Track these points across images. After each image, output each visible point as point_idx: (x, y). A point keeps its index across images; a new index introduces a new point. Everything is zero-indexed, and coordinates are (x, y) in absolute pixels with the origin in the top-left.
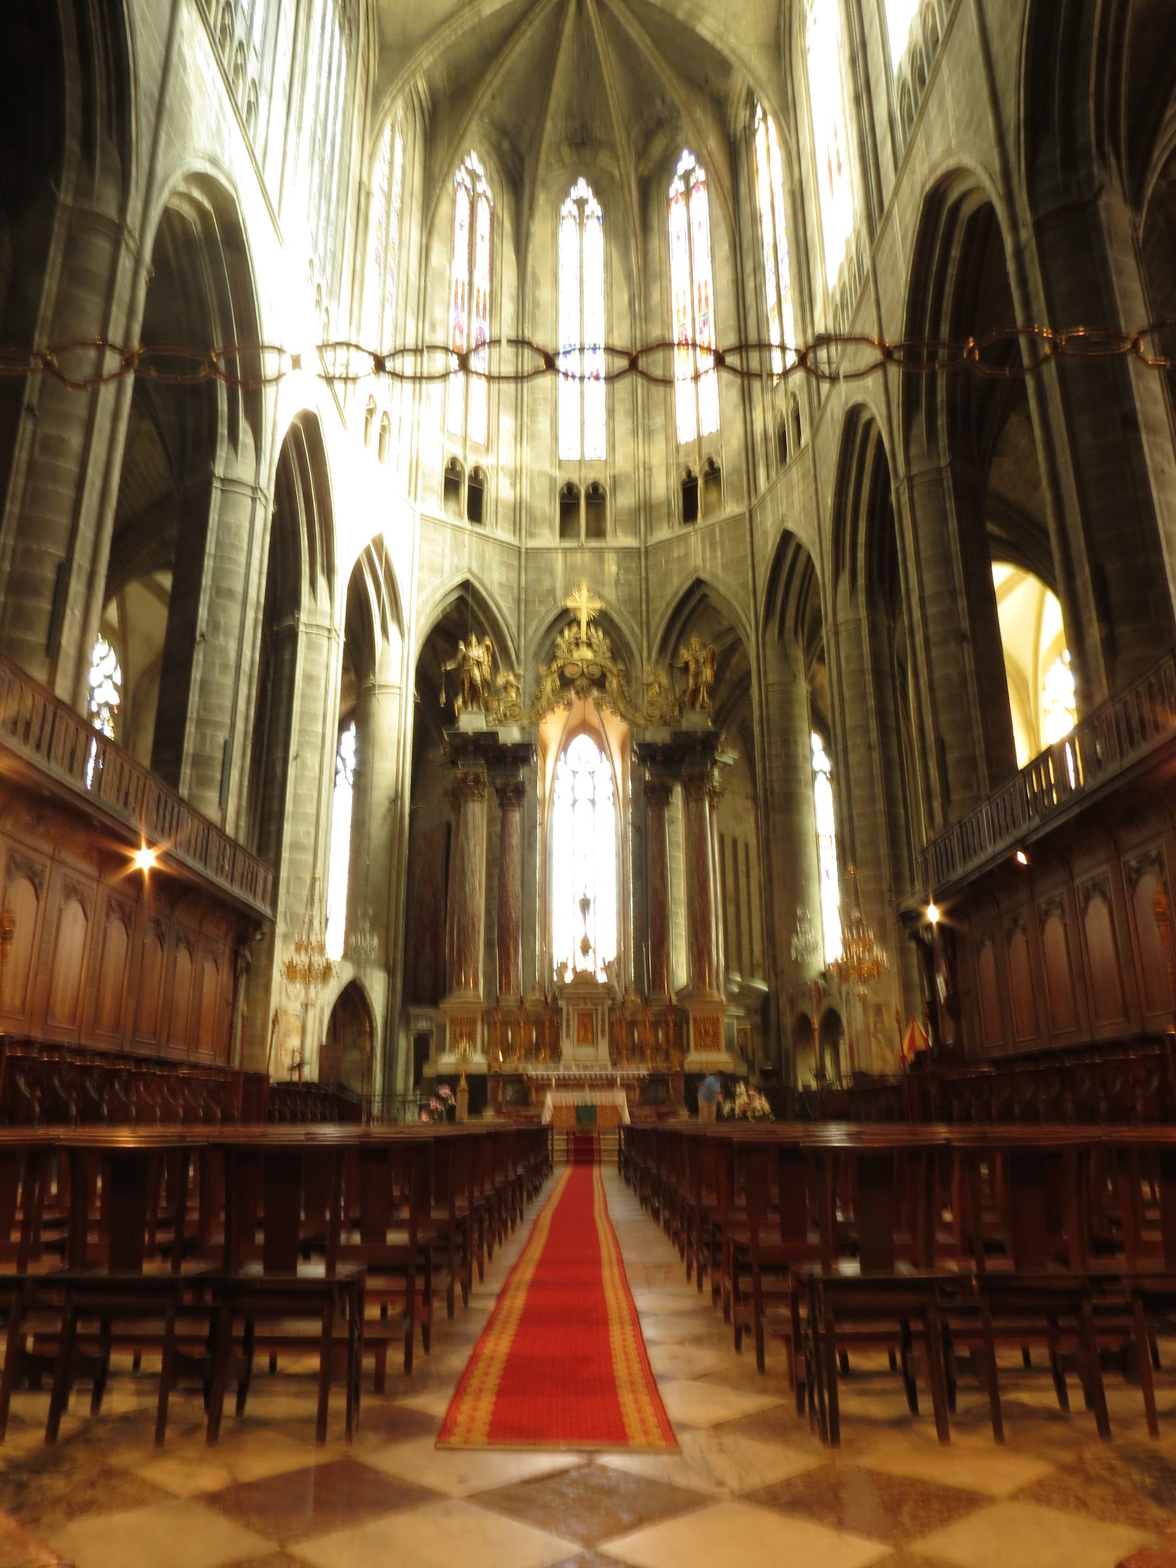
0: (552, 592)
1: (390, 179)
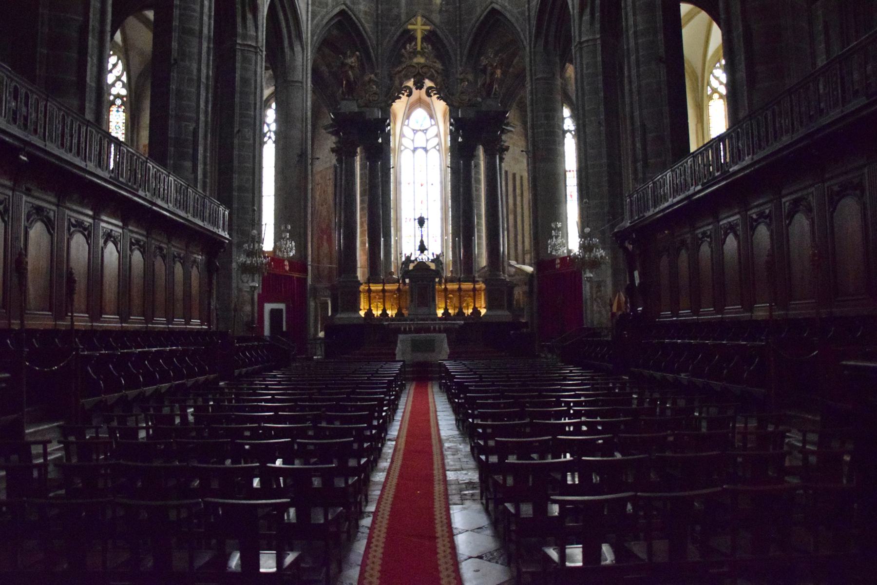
0: (398, 17)
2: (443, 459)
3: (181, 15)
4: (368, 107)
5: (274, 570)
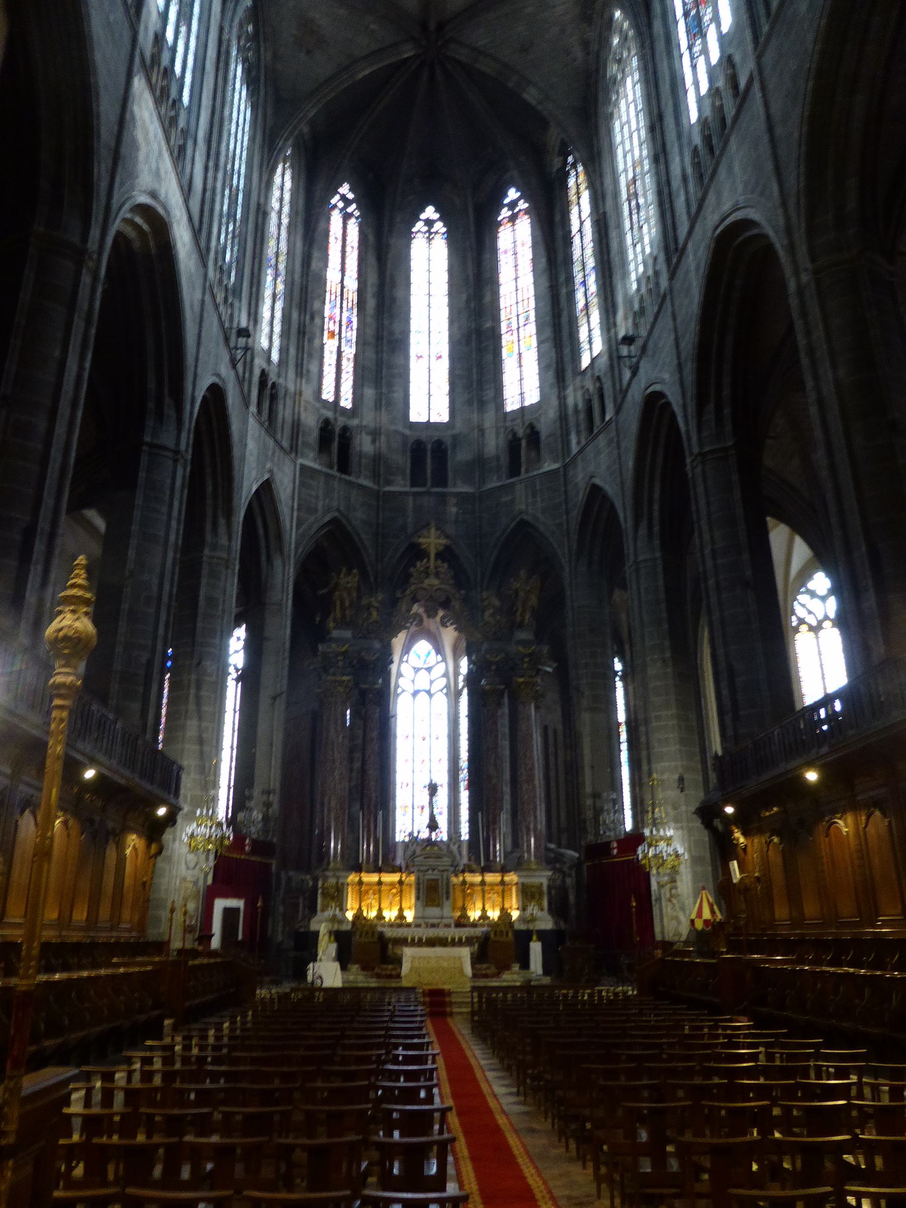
1: (281, 199)
4: (365, 638)
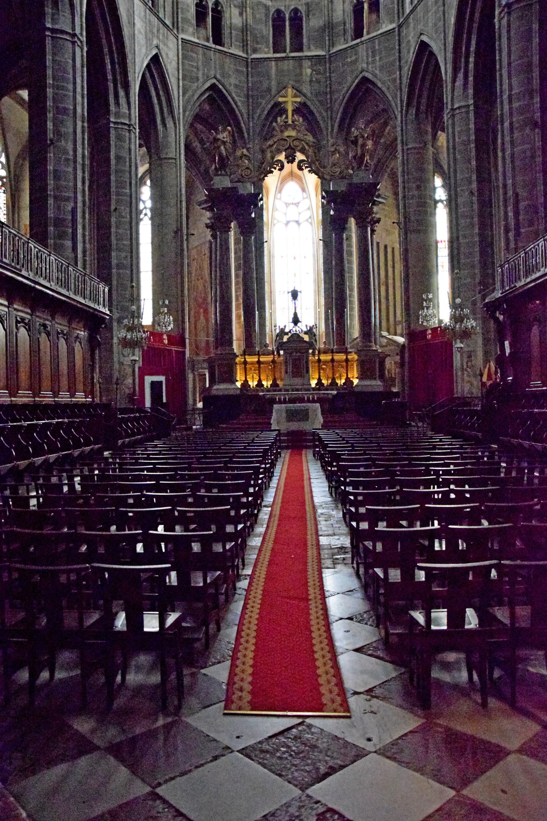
0: (269, 90)
2: (316, 525)
3: (55, 94)
5: (157, 629)
